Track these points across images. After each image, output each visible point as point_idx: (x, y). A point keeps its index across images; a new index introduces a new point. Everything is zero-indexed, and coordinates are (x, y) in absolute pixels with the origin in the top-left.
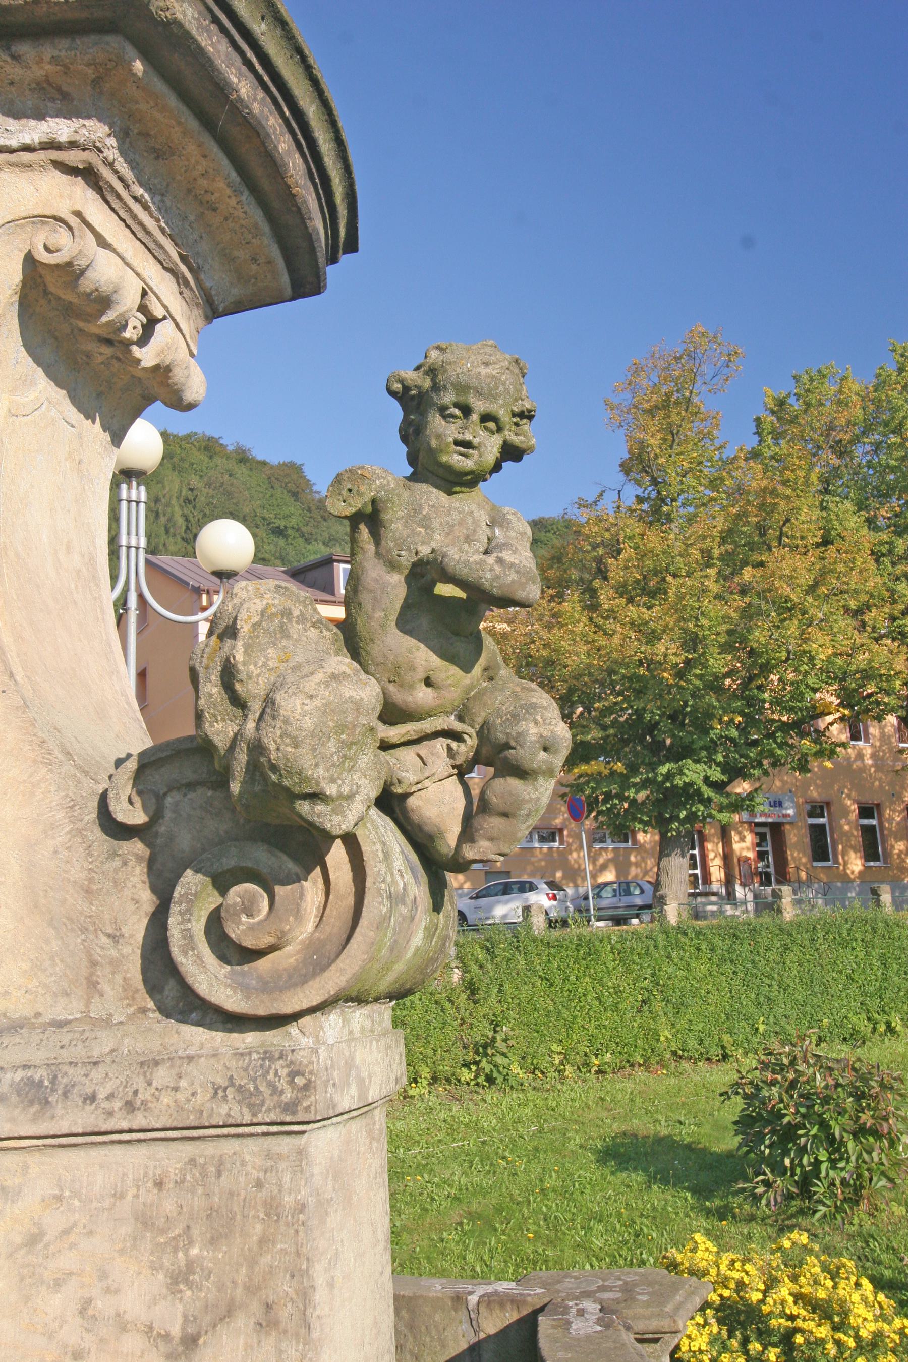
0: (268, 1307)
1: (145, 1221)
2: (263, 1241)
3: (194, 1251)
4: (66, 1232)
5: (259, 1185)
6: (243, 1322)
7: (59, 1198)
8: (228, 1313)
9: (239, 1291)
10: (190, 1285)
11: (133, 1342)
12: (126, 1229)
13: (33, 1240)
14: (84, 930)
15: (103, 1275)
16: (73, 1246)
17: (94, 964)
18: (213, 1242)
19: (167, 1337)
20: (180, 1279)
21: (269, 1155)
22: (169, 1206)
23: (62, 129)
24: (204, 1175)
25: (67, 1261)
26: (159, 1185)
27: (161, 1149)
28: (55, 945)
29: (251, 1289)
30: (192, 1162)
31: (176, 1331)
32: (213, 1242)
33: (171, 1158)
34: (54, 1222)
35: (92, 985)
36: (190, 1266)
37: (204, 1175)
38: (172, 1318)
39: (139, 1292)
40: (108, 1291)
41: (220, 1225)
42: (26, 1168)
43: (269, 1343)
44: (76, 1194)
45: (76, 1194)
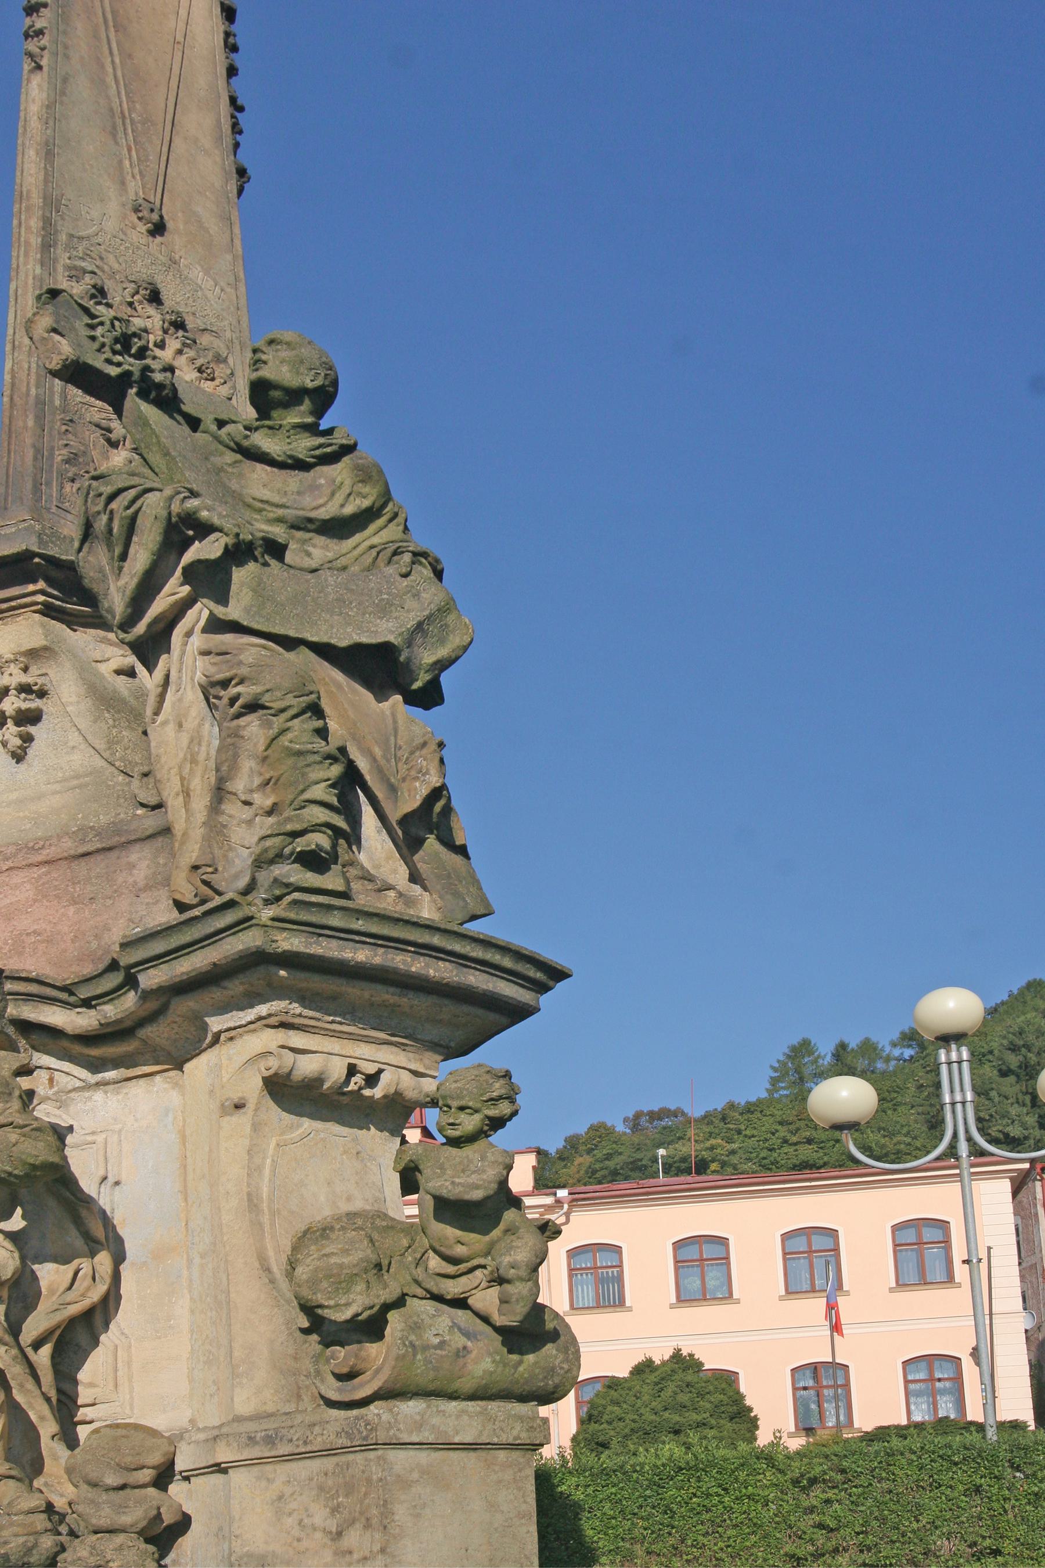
0: (368, 1519)
1: (321, 1488)
2: (366, 1494)
3: (340, 1499)
4: (292, 1494)
5: (363, 1472)
6: (358, 1526)
7: (289, 1482)
8: (353, 1522)
9: (357, 1514)
10: (339, 1512)
11: (318, 1535)
12: (314, 1493)
13: (280, 1498)
14: (295, 1374)
15: (307, 1510)
16: (295, 1500)
17: (299, 1388)
18: (347, 1496)
19: (331, 1533)
20: (335, 1510)
21: (366, 1460)
22: (330, 1483)
23: (263, 1009)
24: (342, 1469)
25: (294, 1505)
26: (326, 1474)
27: (325, 1460)
28: (283, 1382)
29: (361, 1513)
30: (337, 1464)
31: (334, 1530)
32: (347, 1496)
33: (329, 1463)
34: (288, 1491)
35: (299, 1397)
36: (338, 1505)
37: (342, 1469)
38: (332, 1525)
39: (320, 1516)
40: (308, 1516)
41: (349, 1489)
42: (275, 1471)
43: (368, 1534)
44: (295, 1480)
45: (295, 1480)
